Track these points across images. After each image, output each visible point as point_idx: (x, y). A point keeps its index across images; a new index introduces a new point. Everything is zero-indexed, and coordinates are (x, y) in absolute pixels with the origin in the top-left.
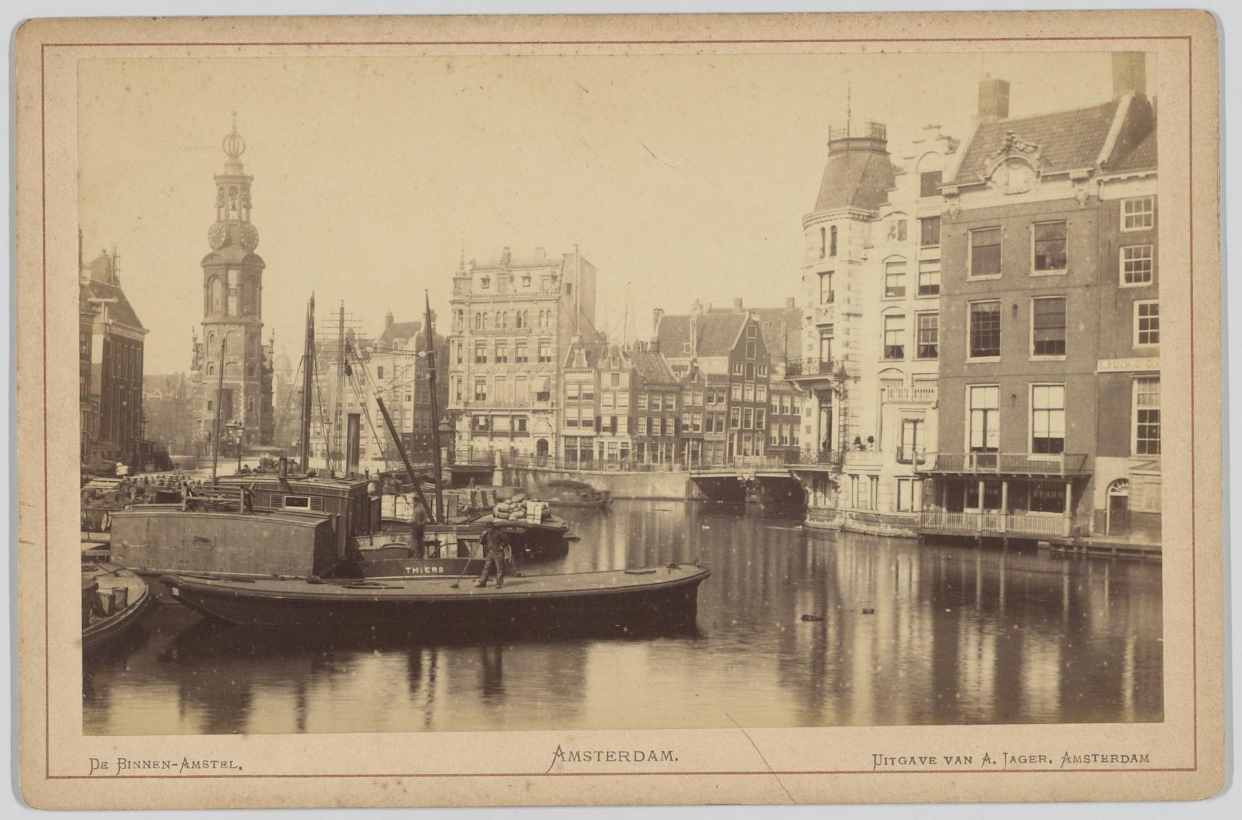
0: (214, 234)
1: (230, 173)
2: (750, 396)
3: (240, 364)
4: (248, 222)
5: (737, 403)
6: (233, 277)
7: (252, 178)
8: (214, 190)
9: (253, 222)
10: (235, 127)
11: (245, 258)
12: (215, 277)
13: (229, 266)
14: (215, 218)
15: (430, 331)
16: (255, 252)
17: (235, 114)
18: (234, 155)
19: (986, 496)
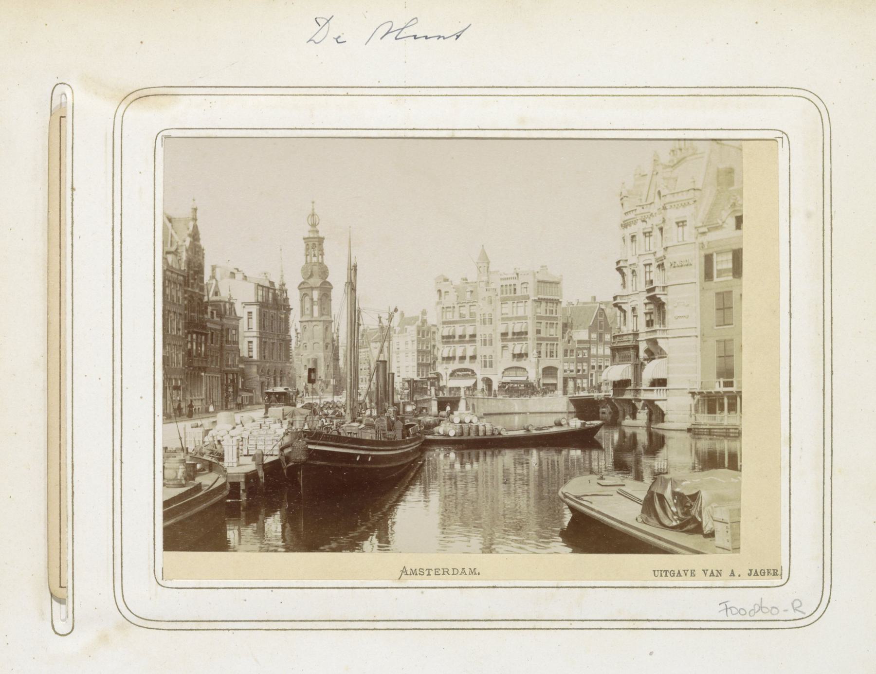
0: (304, 270)
1: (312, 236)
2: (601, 352)
3: (321, 343)
4: (321, 264)
5: (594, 356)
6: (316, 295)
7: (323, 239)
8: (303, 245)
9: (325, 263)
11: (322, 284)
12: (305, 295)
13: (312, 288)
14: (303, 263)
15: (424, 322)
18: (314, 225)
19: (729, 404)
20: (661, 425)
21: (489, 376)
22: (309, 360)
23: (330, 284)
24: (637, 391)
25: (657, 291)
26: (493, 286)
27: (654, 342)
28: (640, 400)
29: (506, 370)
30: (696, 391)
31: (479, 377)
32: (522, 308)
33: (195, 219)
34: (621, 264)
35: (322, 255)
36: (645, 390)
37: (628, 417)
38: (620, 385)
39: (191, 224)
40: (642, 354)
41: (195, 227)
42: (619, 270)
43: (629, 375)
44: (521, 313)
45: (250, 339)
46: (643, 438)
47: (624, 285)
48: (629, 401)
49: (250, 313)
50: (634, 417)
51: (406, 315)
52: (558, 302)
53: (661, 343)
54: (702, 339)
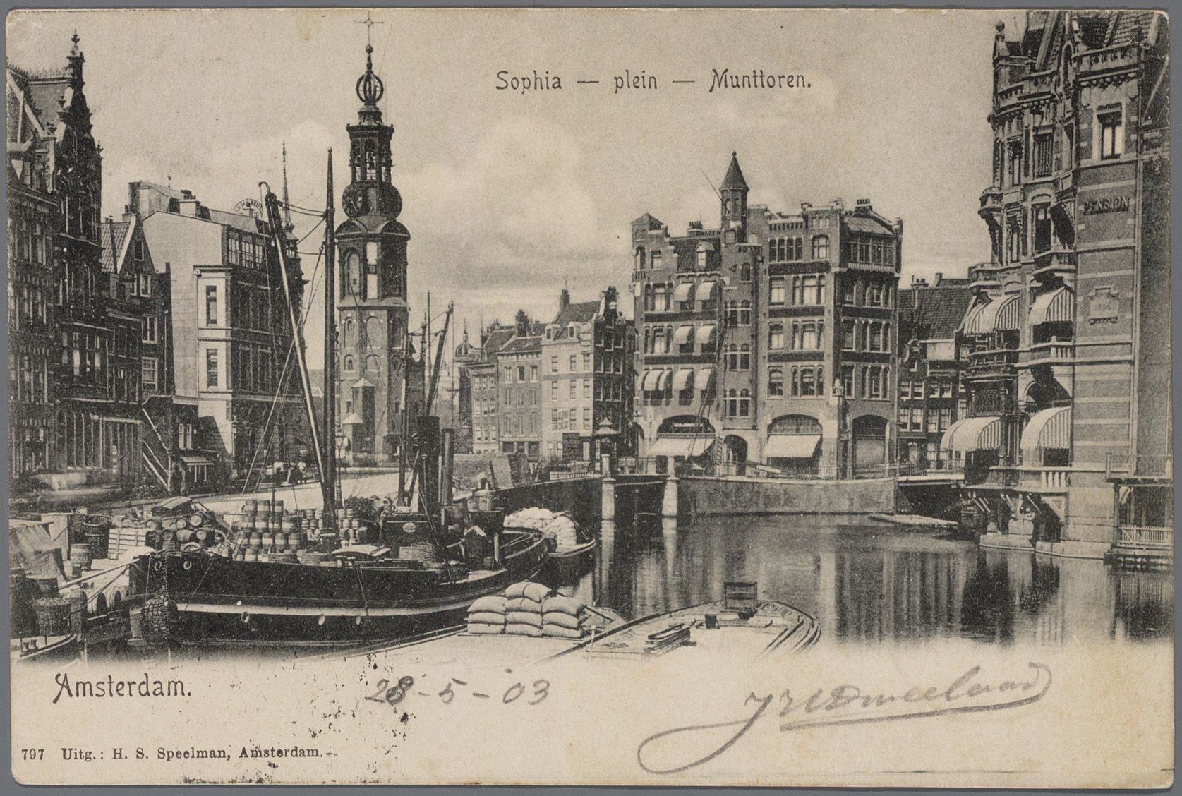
6: (373, 252)
7: (391, 130)
10: (370, 66)
12: (353, 250)
16: (399, 219)
17: (370, 50)
20: (1058, 547)
21: (739, 434)
22: (355, 391)
23: (403, 229)
24: (1012, 475)
25: (1055, 264)
26: (752, 240)
27: (1043, 373)
28: (1014, 494)
29: (775, 421)
30: (1123, 477)
31: (721, 433)
32: (814, 291)
33: (77, 82)
34: (989, 203)
35: (389, 165)
36: (1027, 472)
37: (991, 526)
38: (980, 462)
39: (69, 93)
40: (1023, 396)
41: (79, 100)
42: (987, 215)
43: (994, 443)
44: (810, 298)
45: (211, 345)
46: (1020, 571)
47: (997, 249)
48: (991, 495)
49: (213, 289)
50: (1004, 528)
51: (573, 301)
52: (892, 280)
53: (1062, 377)
54: (1142, 369)
